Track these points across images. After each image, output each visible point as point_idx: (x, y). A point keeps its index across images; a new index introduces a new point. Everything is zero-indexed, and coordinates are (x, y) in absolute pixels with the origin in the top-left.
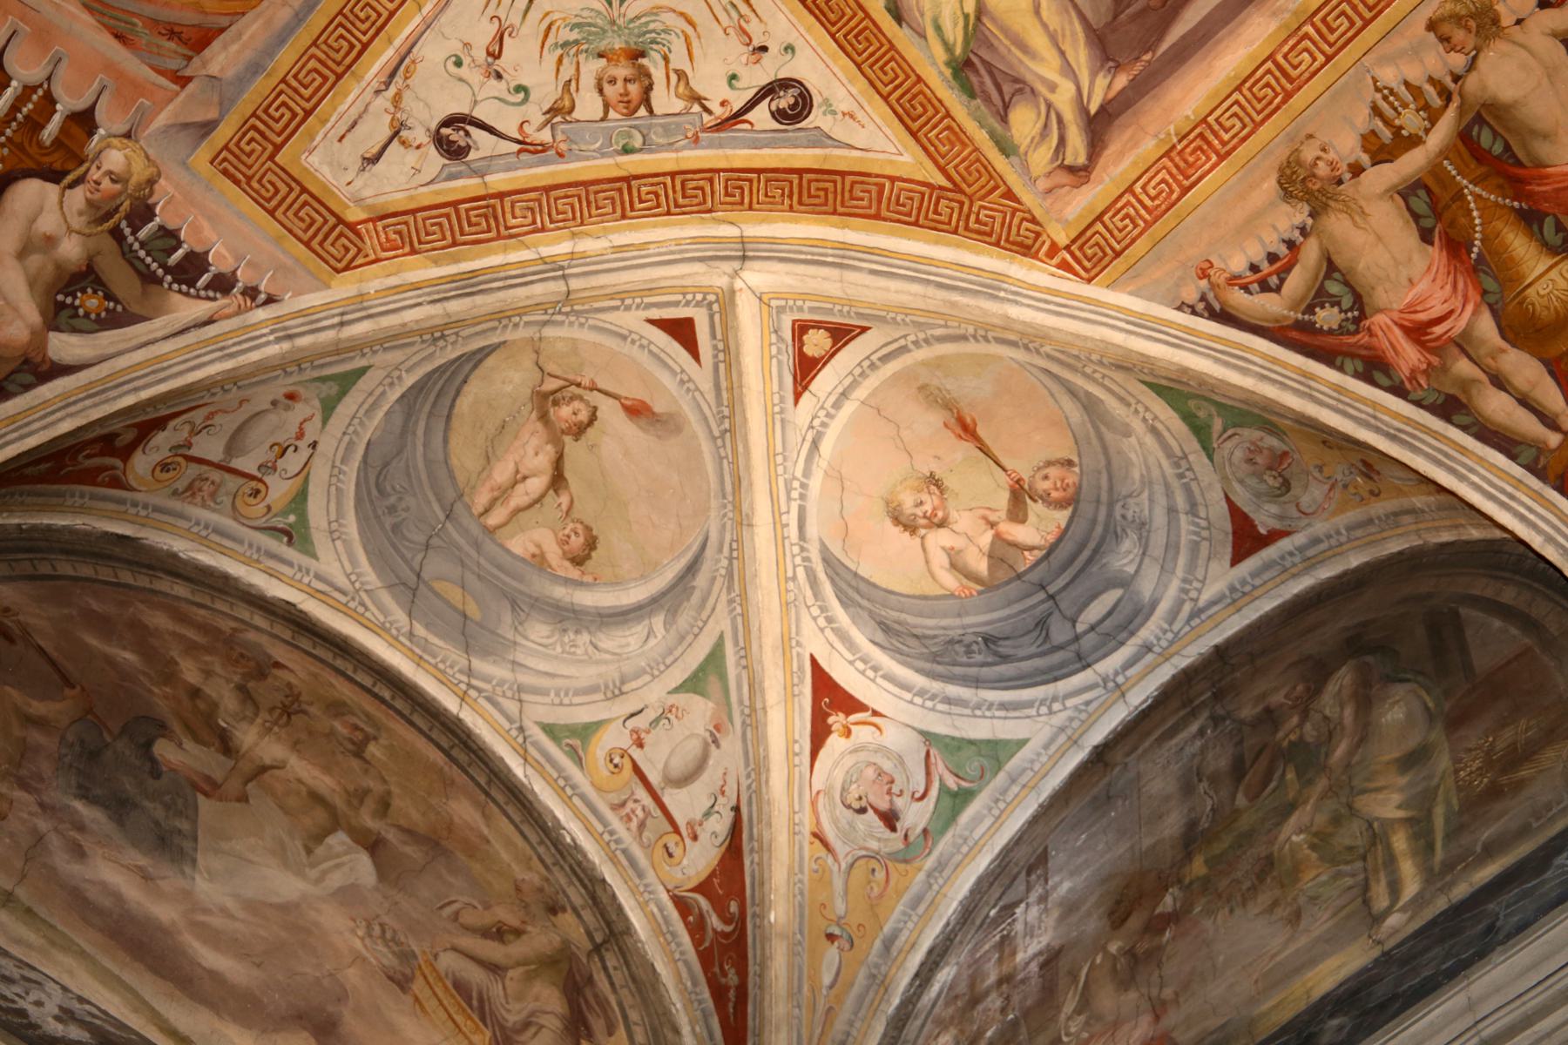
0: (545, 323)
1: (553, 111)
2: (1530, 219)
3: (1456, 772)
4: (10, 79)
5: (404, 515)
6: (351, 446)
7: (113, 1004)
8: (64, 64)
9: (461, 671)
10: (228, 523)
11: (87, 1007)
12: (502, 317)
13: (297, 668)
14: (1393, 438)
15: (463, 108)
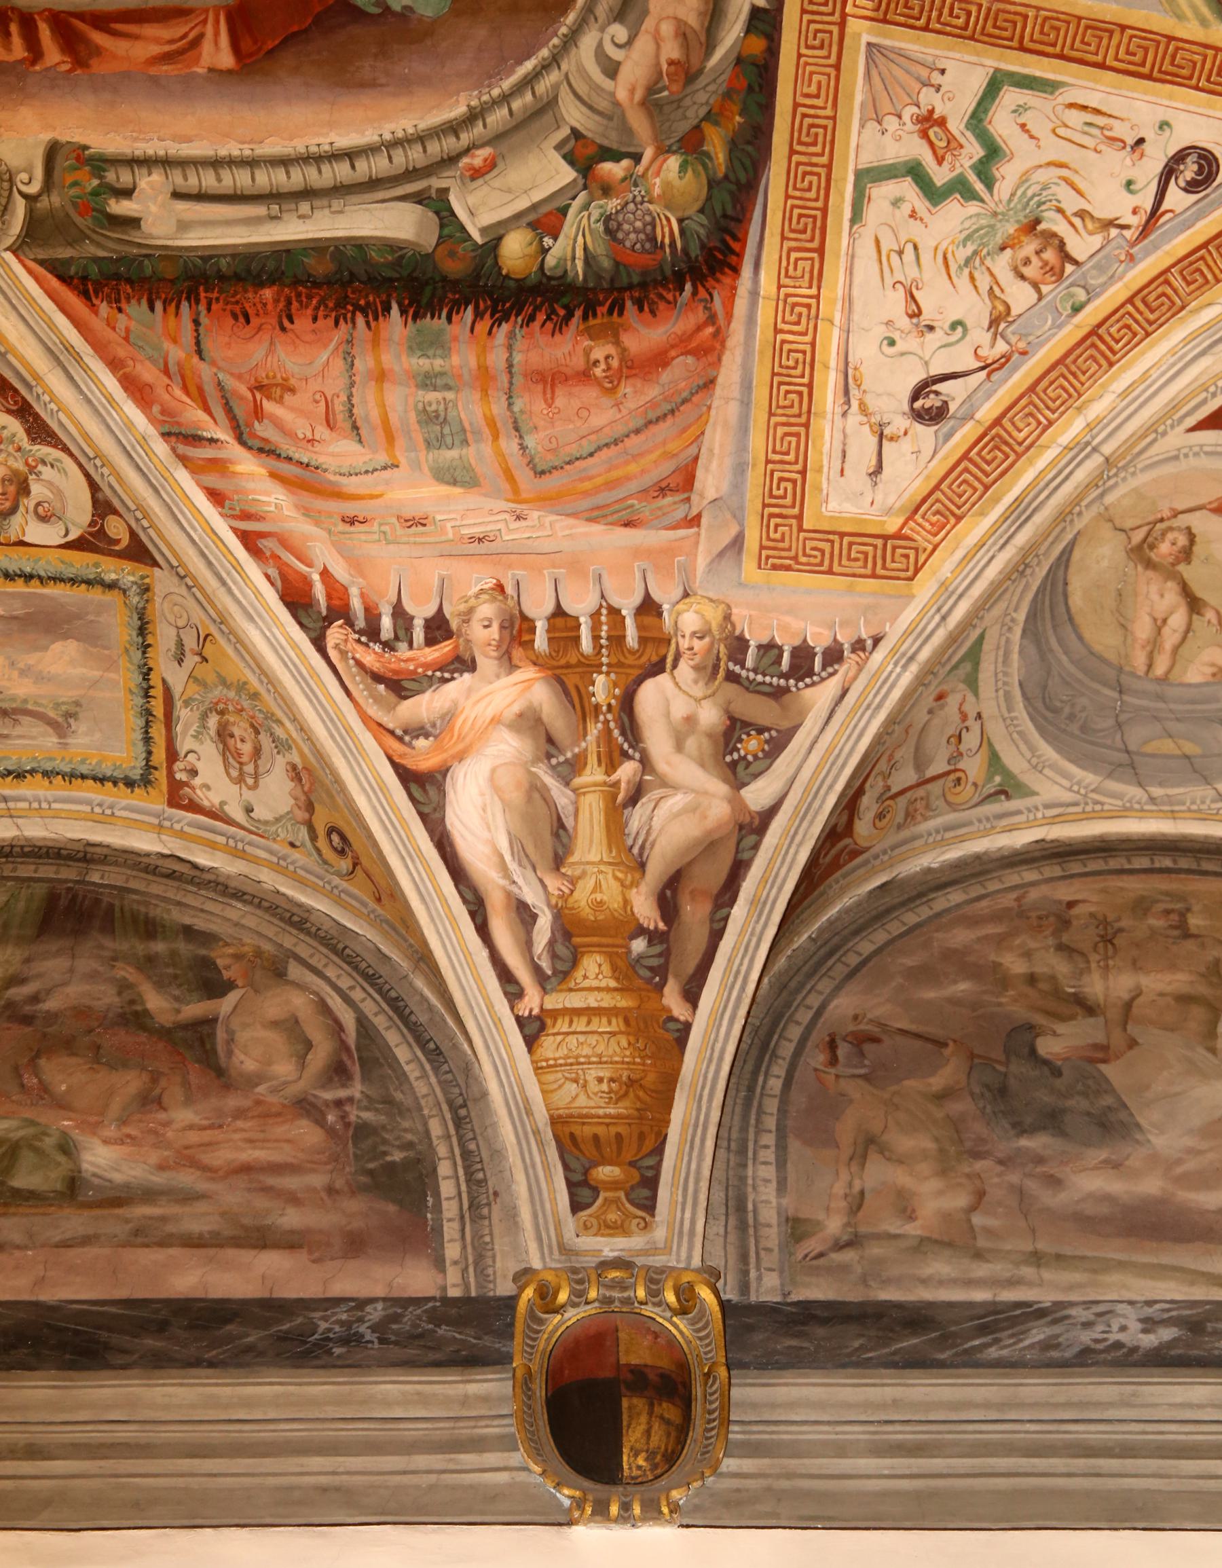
0: (1102, 495)
1: (994, 322)
4: (577, 618)
5: (1084, 715)
6: (1008, 697)
7: (1171, 1290)
8: (605, 577)
9: (1213, 801)
10: (951, 817)
11: (1157, 1306)
12: (1064, 516)
13: (1087, 894)
15: (921, 376)
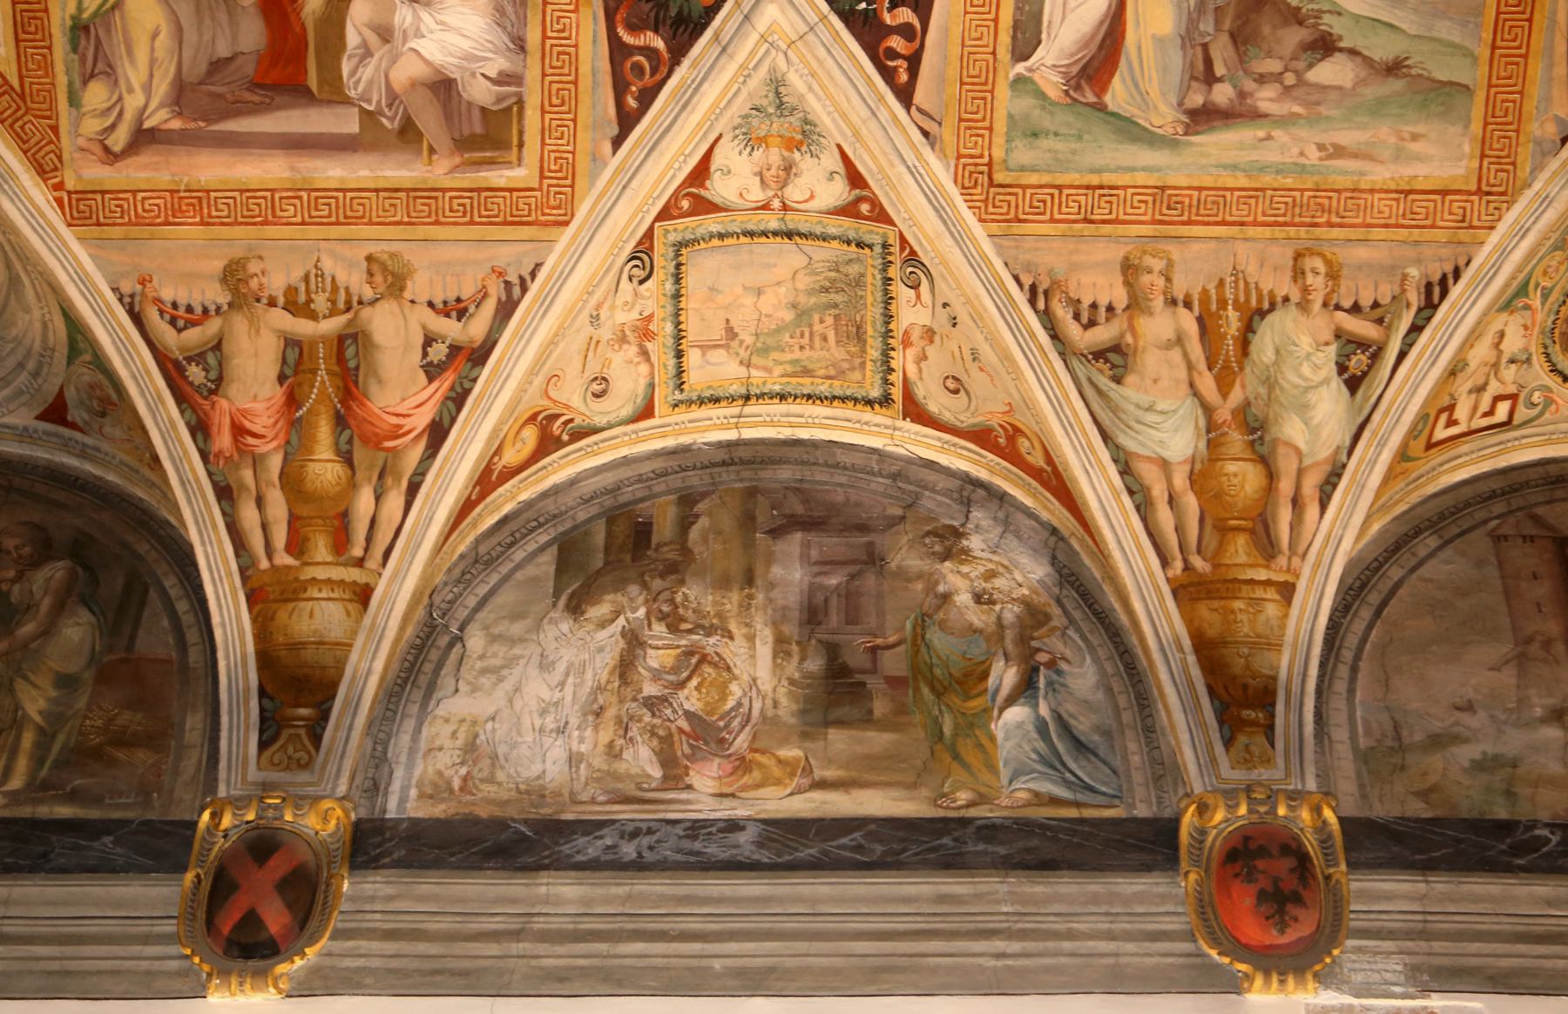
2: (340, 422)
3: (86, 717)
14: (183, 483)
